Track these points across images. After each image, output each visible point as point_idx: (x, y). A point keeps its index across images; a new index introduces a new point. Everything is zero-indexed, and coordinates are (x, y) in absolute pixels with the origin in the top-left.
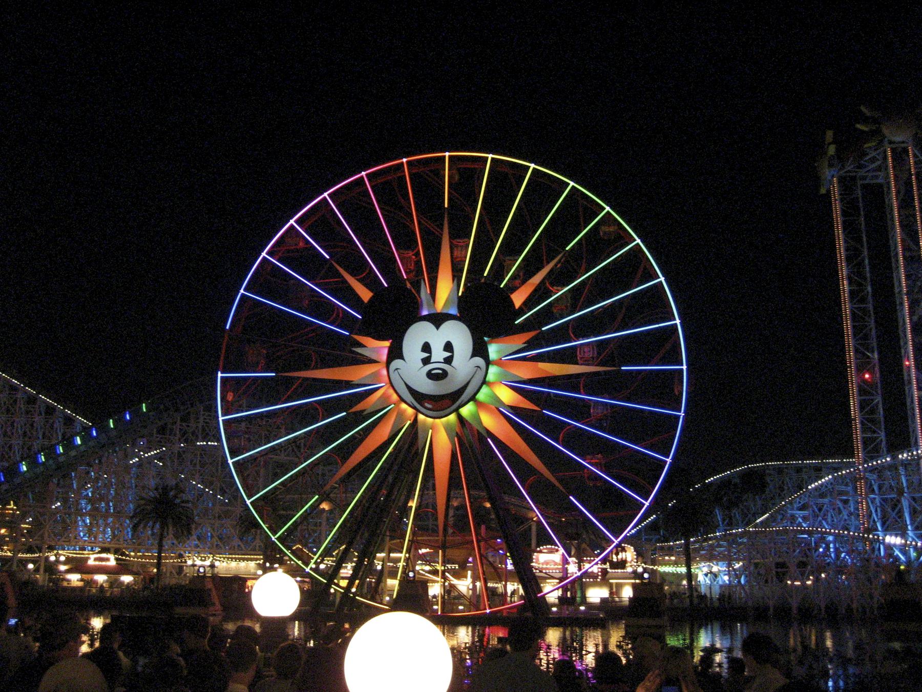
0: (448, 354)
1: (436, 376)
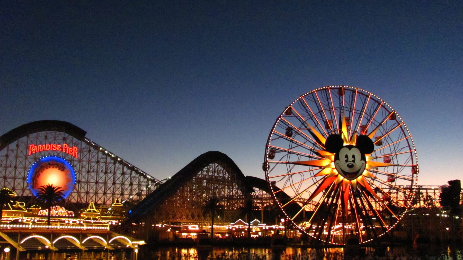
0: (353, 159)
1: (351, 166)
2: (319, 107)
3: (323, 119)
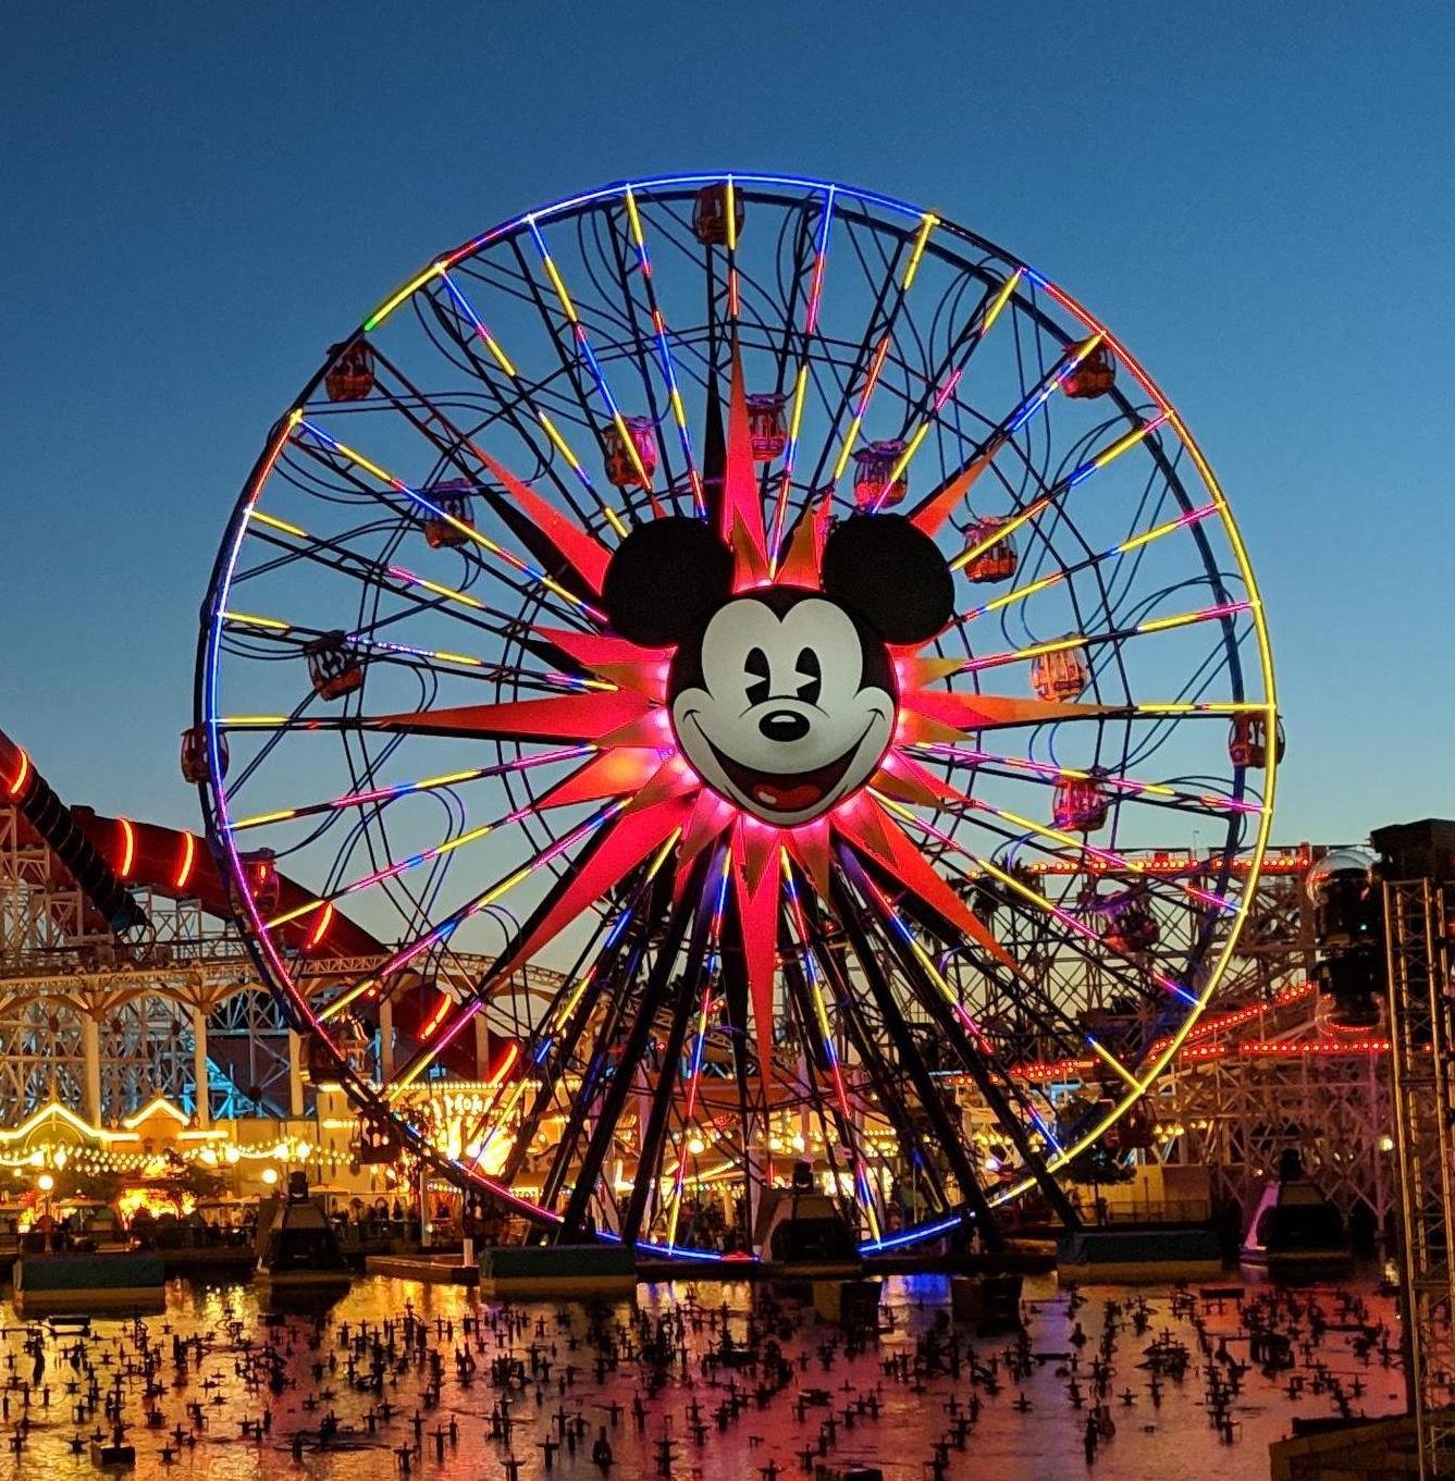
2: (561, 336)
3: (589, 413)
